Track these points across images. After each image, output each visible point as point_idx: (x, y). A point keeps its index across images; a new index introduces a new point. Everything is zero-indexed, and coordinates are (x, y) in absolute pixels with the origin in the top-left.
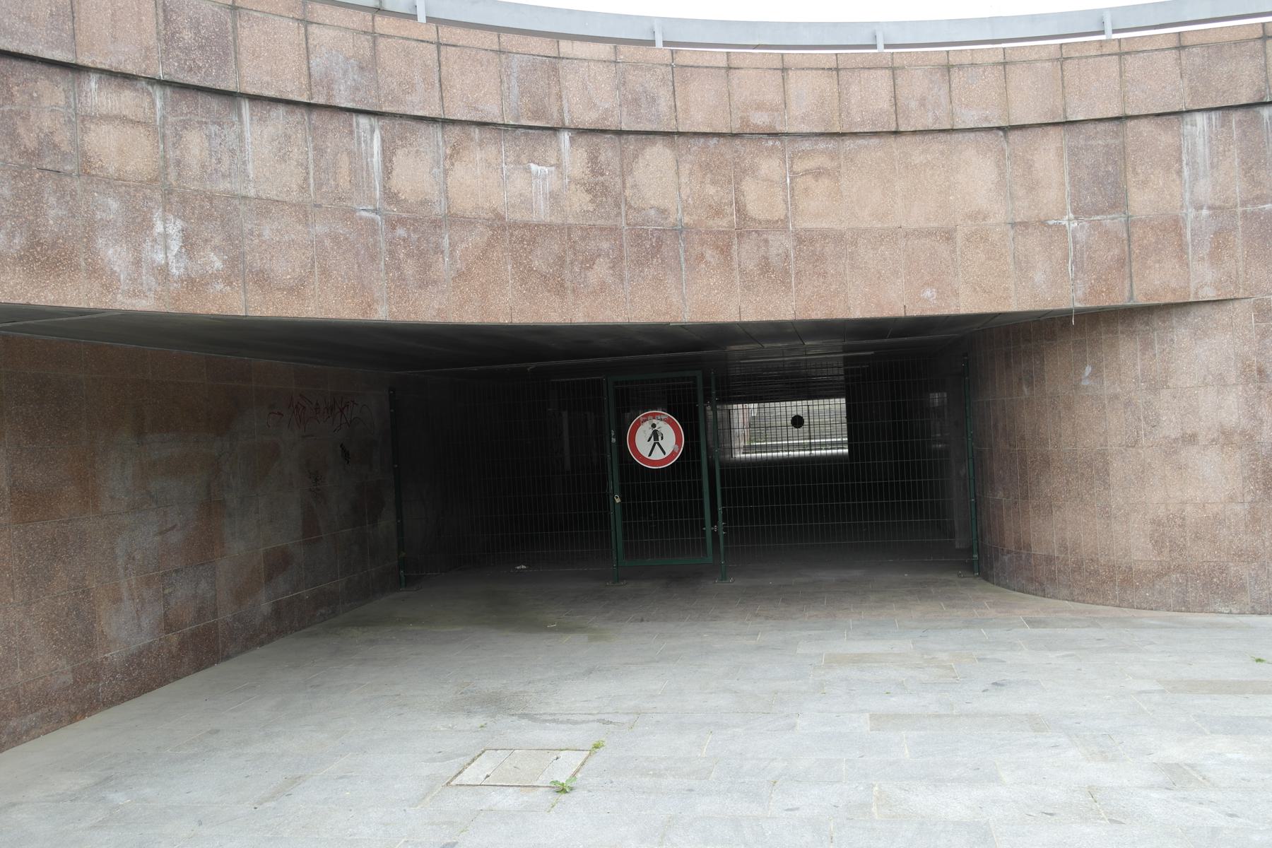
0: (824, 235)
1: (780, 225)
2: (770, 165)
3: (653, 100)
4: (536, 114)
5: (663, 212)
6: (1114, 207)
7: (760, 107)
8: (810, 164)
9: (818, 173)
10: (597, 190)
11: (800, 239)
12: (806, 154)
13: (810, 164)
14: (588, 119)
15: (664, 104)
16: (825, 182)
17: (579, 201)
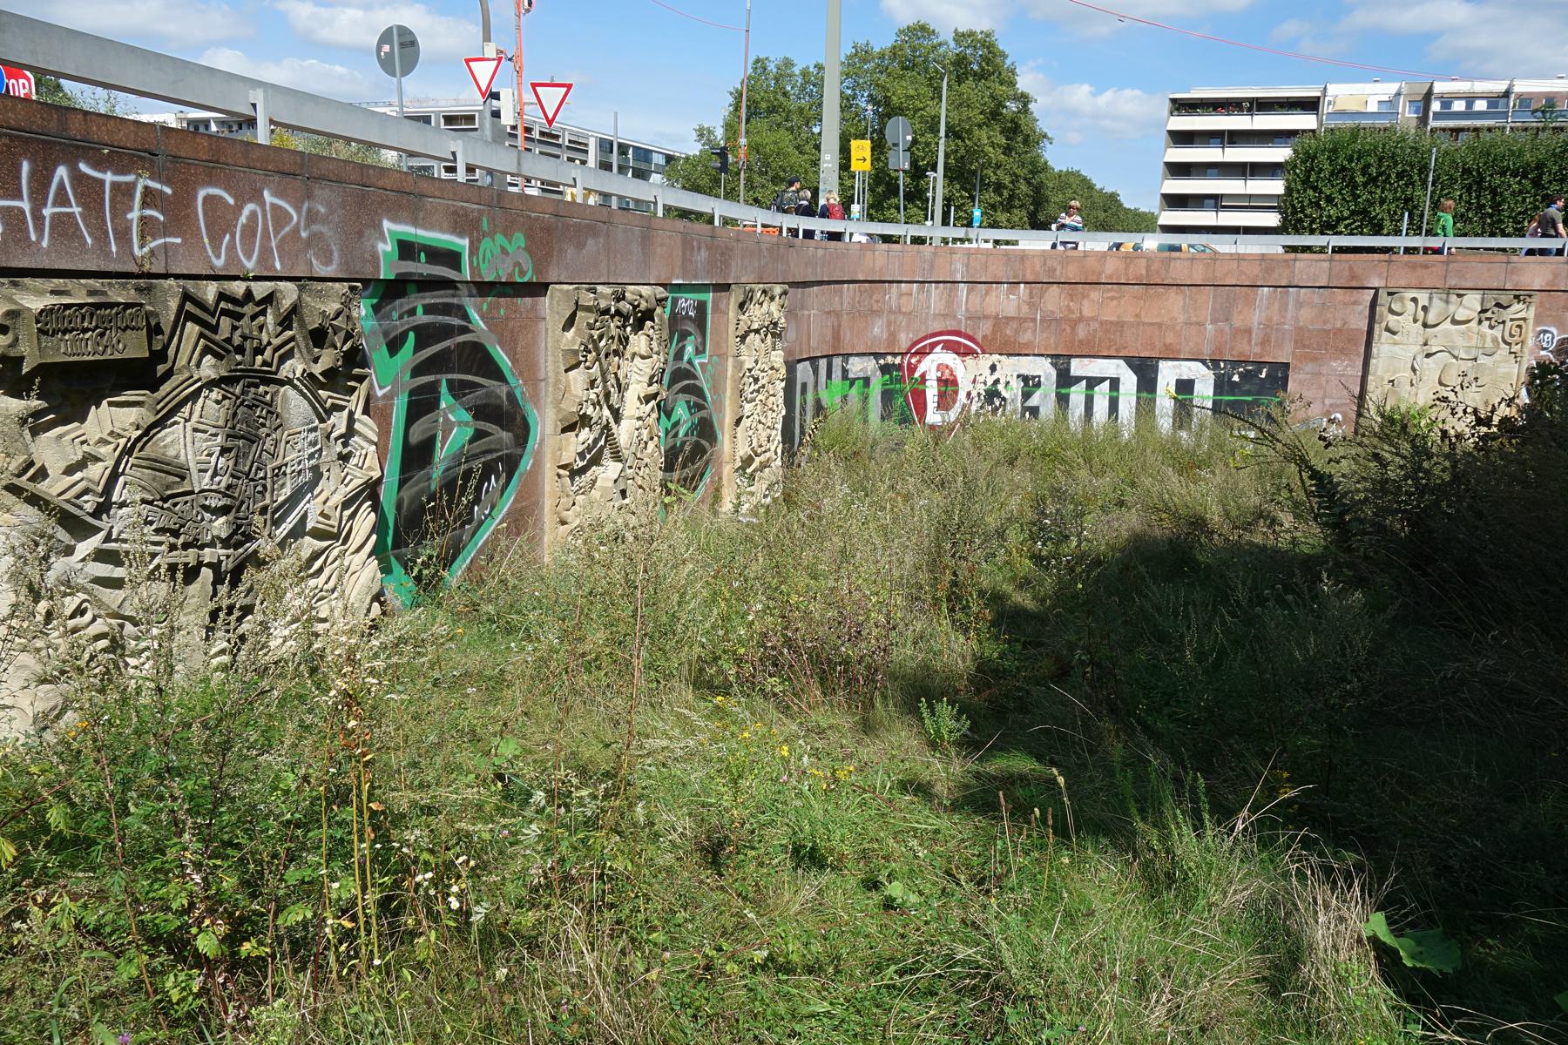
0: (1112, 323)
1: (1094, 319)
2: (1095, 294)
3: (1055, 270)
4: (1014, 277)
5: (1053, 312)
6: (1227, 320)
7: (1094, 272)
8: (1110, 295)
9: (1112, 298)
10: (1031, 304)
11: (1102, 323)
12: (1109, 290)
13: (1110, 295)
14: (1030, 279)
15: (1058, 272)
16: (1115, 302)
17: (1025, 308)
